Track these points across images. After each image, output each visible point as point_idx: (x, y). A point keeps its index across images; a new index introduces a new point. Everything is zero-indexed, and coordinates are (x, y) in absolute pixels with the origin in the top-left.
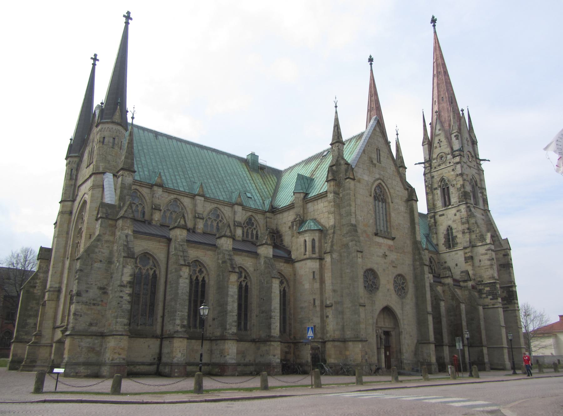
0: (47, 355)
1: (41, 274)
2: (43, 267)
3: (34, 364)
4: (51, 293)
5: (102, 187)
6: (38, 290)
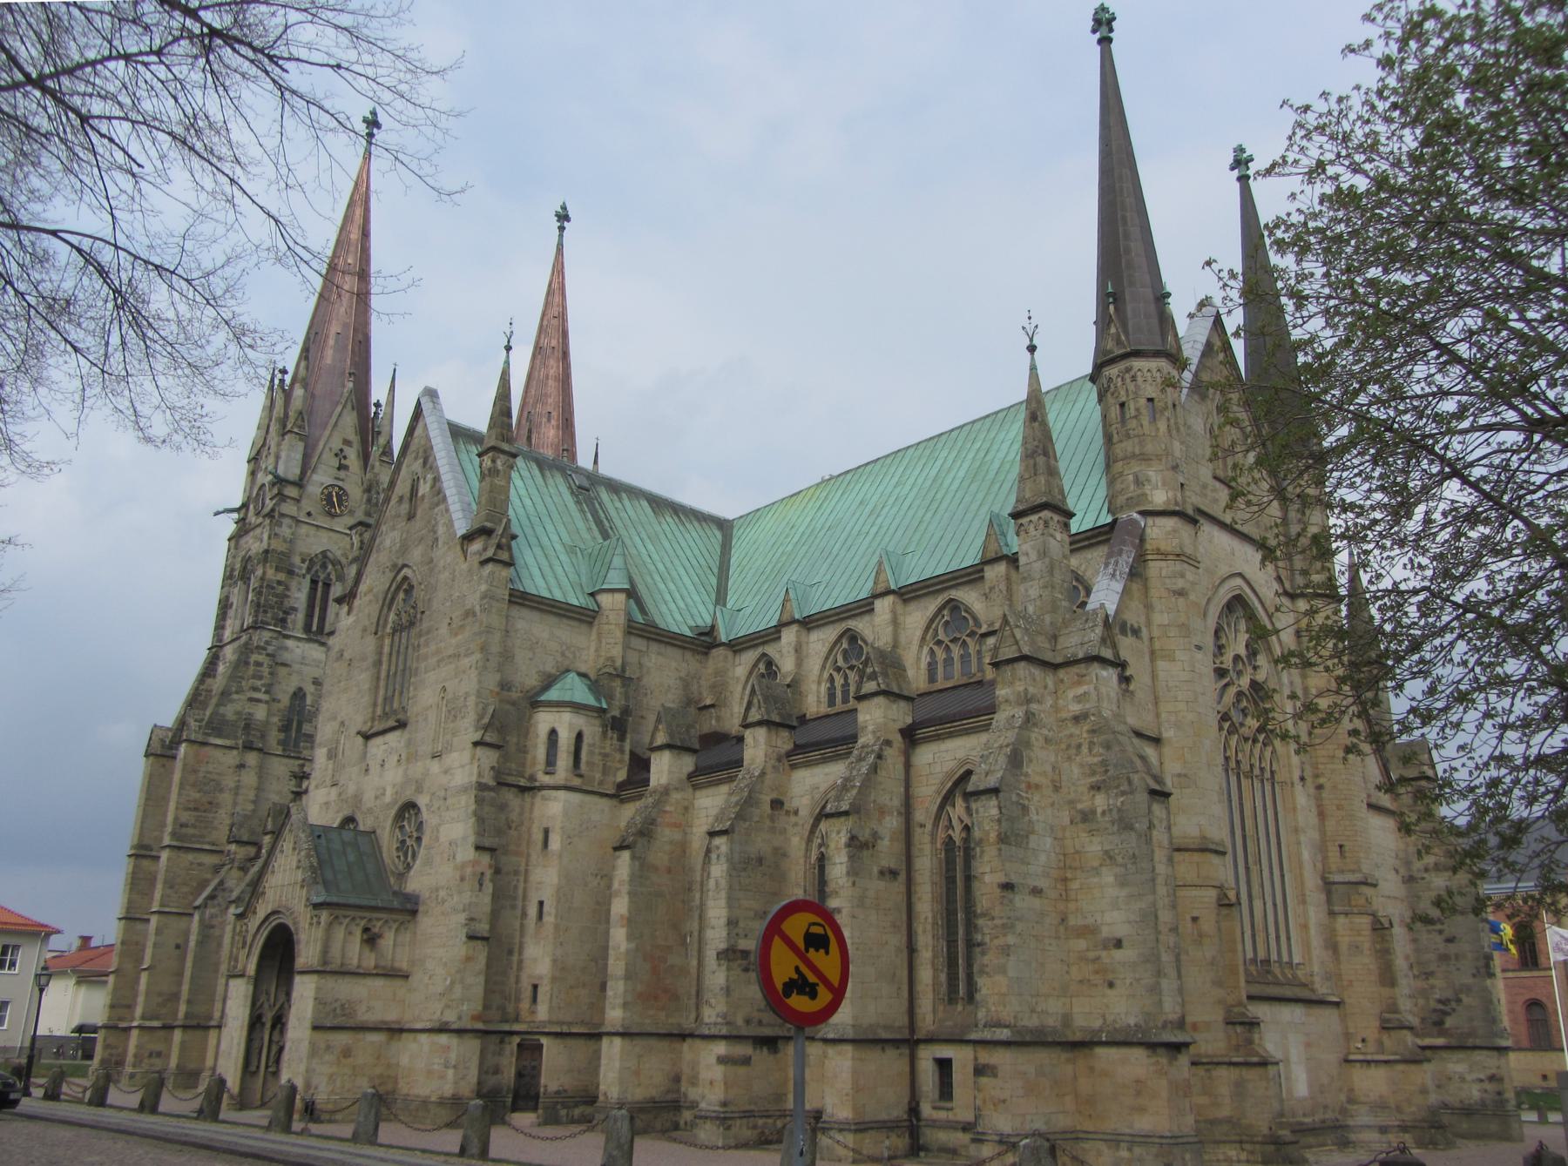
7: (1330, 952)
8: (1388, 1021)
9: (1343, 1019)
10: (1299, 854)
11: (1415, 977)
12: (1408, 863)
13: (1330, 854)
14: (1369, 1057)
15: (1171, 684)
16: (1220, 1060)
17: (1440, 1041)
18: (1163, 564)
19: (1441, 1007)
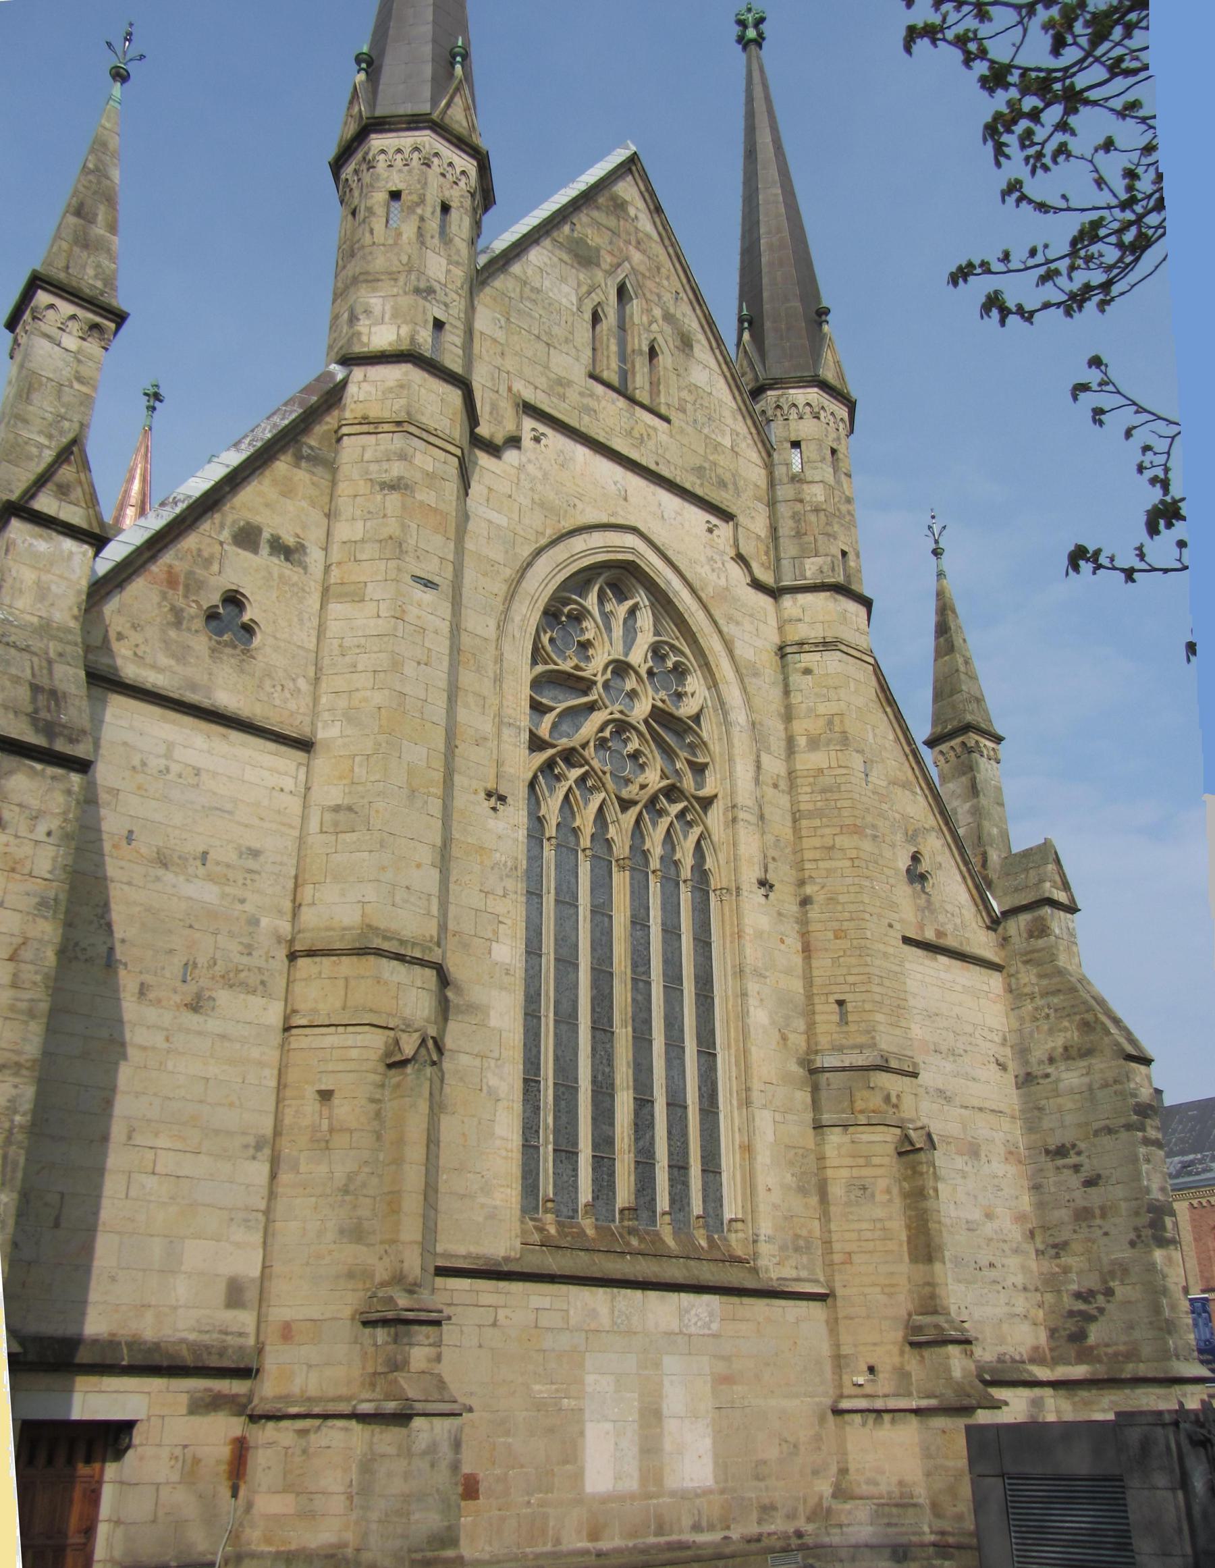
7: (814, 1200)
8: (917, 1329)
9: (833, 1326)
10: (744, 1015)
11: (1037, 1251)
12: (1022, 1052)
13: (818, 1018)
14: (879, 1404)
15: (347, 642)
16: (332, 1408)
17: (1079, 1371)
18: (372, 438)
19: (1080, 1306)
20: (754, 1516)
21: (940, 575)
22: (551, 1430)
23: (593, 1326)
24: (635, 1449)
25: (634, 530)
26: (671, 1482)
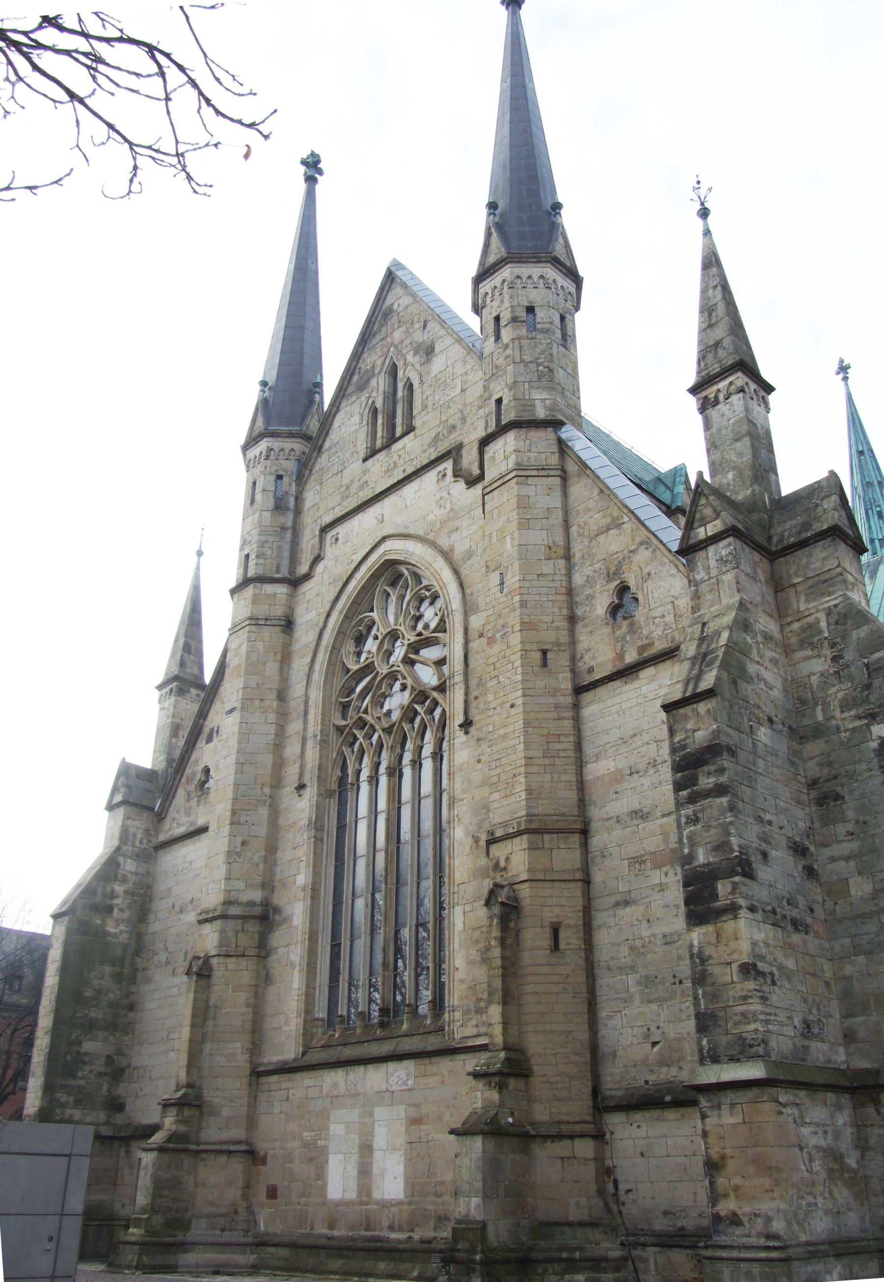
0: (234, 1194)
1: (129, 861)
2: (134, 835)
3: (180, 1237)
4: (231, 923)
5: (559, 473)
6: (118, 922)
20: (432, 1223)
21: (707, 233)
22: (311, 1160)
23: (335, 1094)
24: (356, 1172)
25: (384, 539)
26: (377, 1195)
